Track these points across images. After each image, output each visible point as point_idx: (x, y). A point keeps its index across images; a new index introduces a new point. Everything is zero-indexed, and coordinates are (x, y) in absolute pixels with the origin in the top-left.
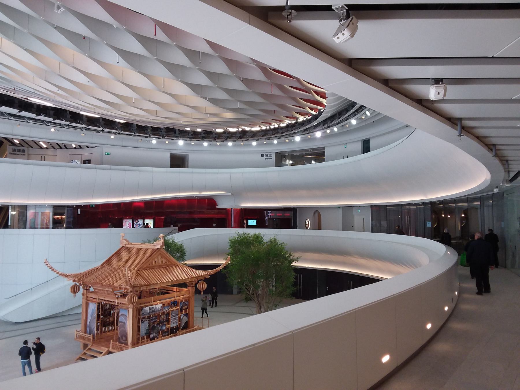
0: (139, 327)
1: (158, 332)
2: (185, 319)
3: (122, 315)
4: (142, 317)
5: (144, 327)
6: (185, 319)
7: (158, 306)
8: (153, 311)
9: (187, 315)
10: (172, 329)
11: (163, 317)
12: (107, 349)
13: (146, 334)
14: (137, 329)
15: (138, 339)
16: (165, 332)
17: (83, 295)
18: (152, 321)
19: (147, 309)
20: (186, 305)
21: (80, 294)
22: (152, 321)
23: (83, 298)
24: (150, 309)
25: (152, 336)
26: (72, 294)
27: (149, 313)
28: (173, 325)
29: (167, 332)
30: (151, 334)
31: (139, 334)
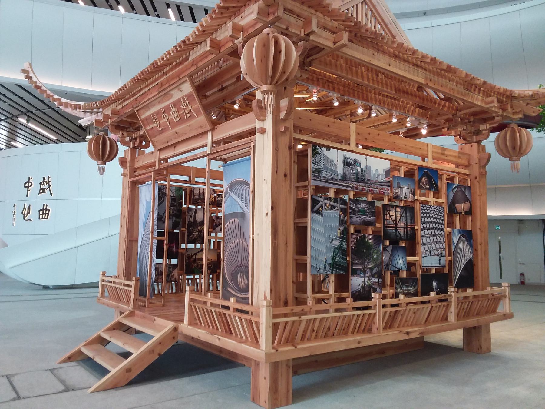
0: (301, 233)
1: (380, 275)
2: (465, 252)
3: (232, 186)
4: (313, 183)
5: (324, 233)
6: (465, 252)
7: (377, 166)
8: (358, 178)
9: (468, 235)
10: (427, 277)
11: (395, 215)
12: (169, 325)
13: (334, 265)
14: (295, 240)
15: (301, 287)
16: (404, 282)
17: (123, 162)
18: (357, 219)
19: (335, 157)
20: (466, 200)
21: (114, 166)
22: (357, 219)
23: (124, 175)
24: (347, 164)
25: (357, 282)
26: (94, 164)
27: (344, 178)
28: (429, 259)
29: (411, 279)
30: (354, 272)
31: (301, 267)
